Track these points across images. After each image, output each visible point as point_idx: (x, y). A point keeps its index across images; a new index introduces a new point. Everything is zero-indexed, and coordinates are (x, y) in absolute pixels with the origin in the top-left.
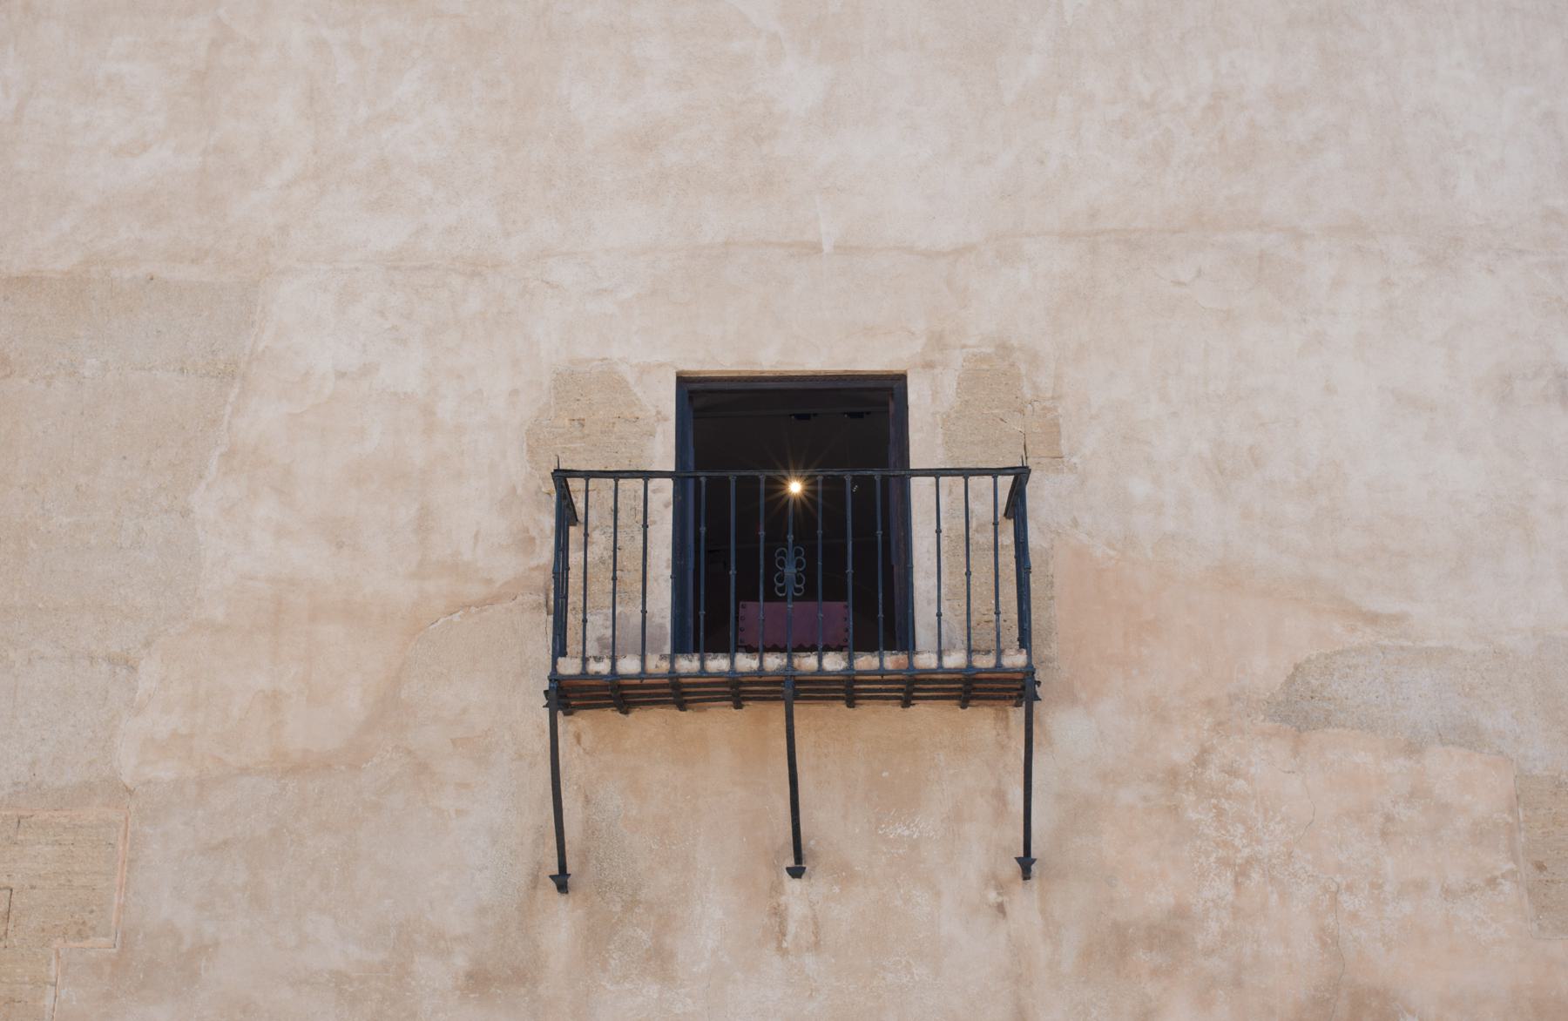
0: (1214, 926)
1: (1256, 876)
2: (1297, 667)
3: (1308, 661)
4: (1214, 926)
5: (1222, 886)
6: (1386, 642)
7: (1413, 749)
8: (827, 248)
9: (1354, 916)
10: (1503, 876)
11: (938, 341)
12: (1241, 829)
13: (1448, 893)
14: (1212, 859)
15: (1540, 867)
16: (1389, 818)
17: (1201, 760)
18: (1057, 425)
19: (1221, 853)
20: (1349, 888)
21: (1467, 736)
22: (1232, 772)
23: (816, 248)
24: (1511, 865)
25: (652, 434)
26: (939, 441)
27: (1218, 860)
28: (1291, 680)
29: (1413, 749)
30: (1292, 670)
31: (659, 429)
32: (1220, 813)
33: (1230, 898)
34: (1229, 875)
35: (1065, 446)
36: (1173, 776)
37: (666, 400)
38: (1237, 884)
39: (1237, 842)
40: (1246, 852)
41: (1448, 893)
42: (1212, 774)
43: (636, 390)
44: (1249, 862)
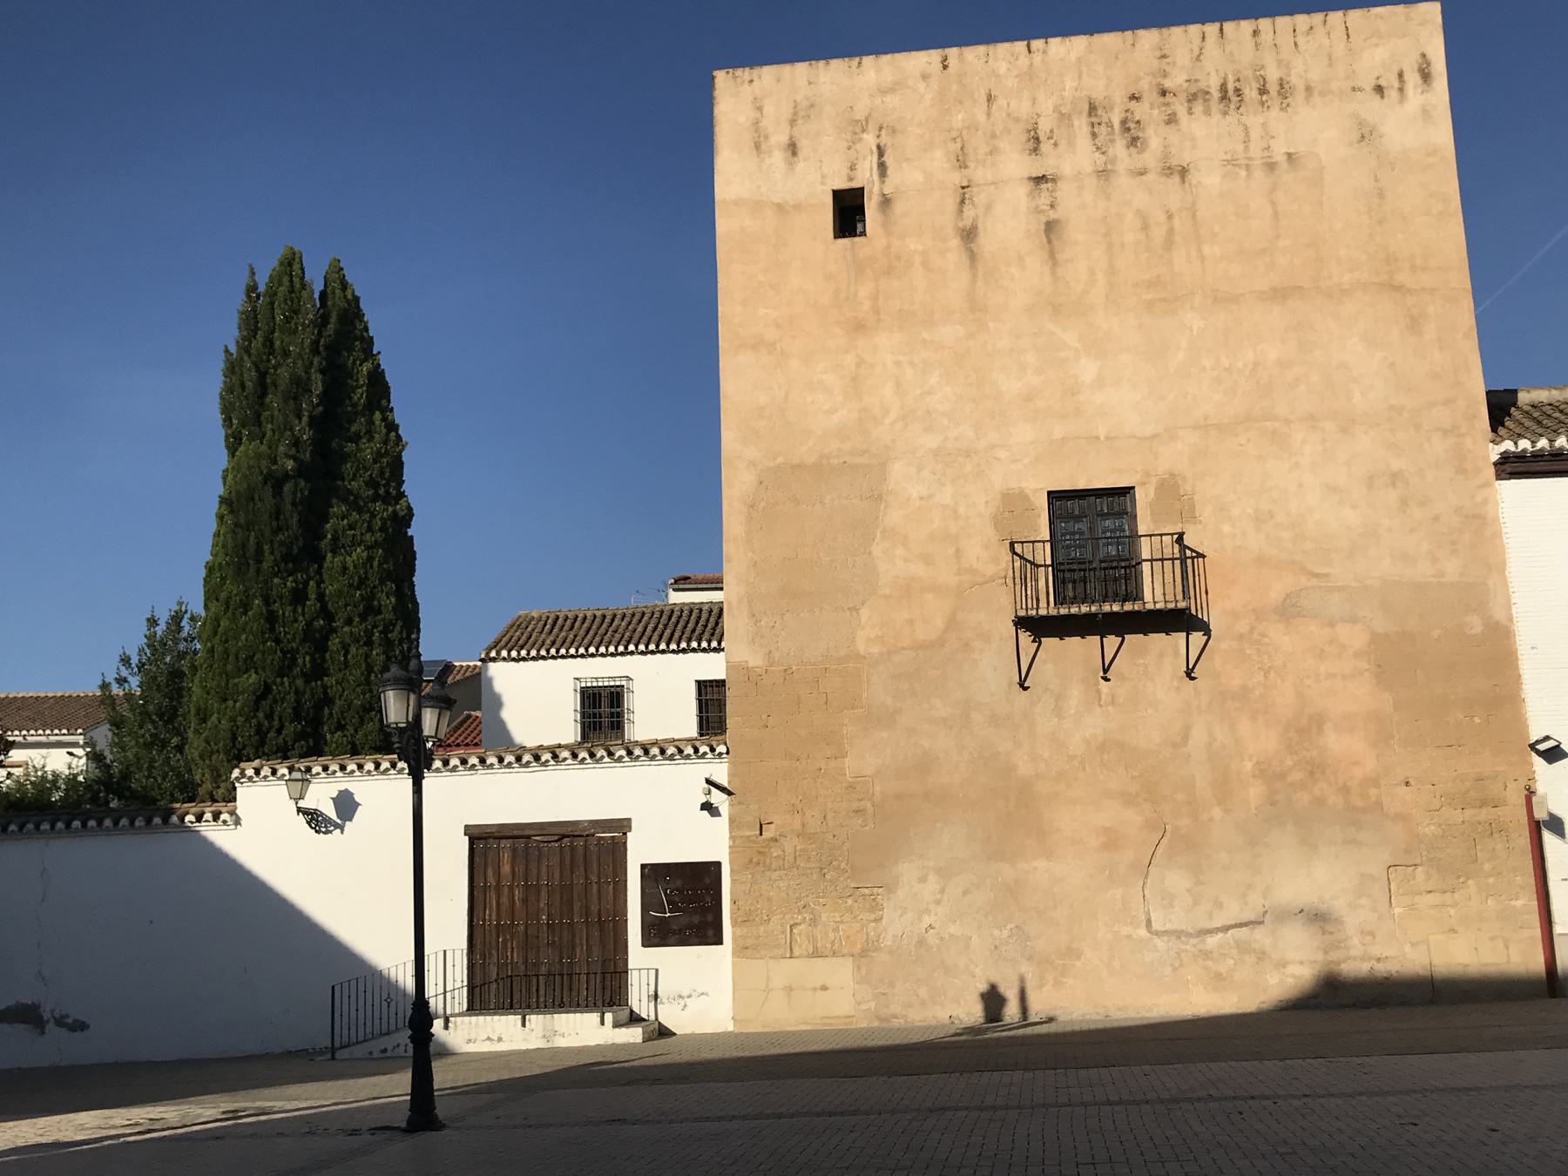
0: (1257, 693)
1: (1272, 672)
2: (1287, 595)
3: (1292, 592)
4: (1257, 693)
5: (1260, 677)
6: (1322, 584)
7: (1331, 625)
8: (1102, 439)
9: (1309, 686)
10: (1366, 670)
11: (1147, 474)
12: (1266, 656)
13: (1344, 677)
14: (1256, 667)
15: (1379, 666)
16: (1322, 651)
17: (1252, 629)
18: (1194, 506)
19: (1260, 665)
20: (1307, 677)
21: (1354, 620)
22: (1264, 635)
23: (1098, 438)
24: (1368, 667)
25: (1040, 516)
26: (1149, 513)
27: (1258, 668)
28: (1285, 599)
29: (1331, 625)
30: (1285, 596)
31: (1042, 515)
32: (1259, 651)
33: (1263, 682)
34: (1262, 673)
35: (1197, 514)
36: (1241, 637)
37: (1042, 502)
38: (1265, 677)
39: (1266, 661)
40: (1269, 664)
41: (1344, 677)
42: (1256, 636)
43: (1032, 499)
44: (1270, 667)
